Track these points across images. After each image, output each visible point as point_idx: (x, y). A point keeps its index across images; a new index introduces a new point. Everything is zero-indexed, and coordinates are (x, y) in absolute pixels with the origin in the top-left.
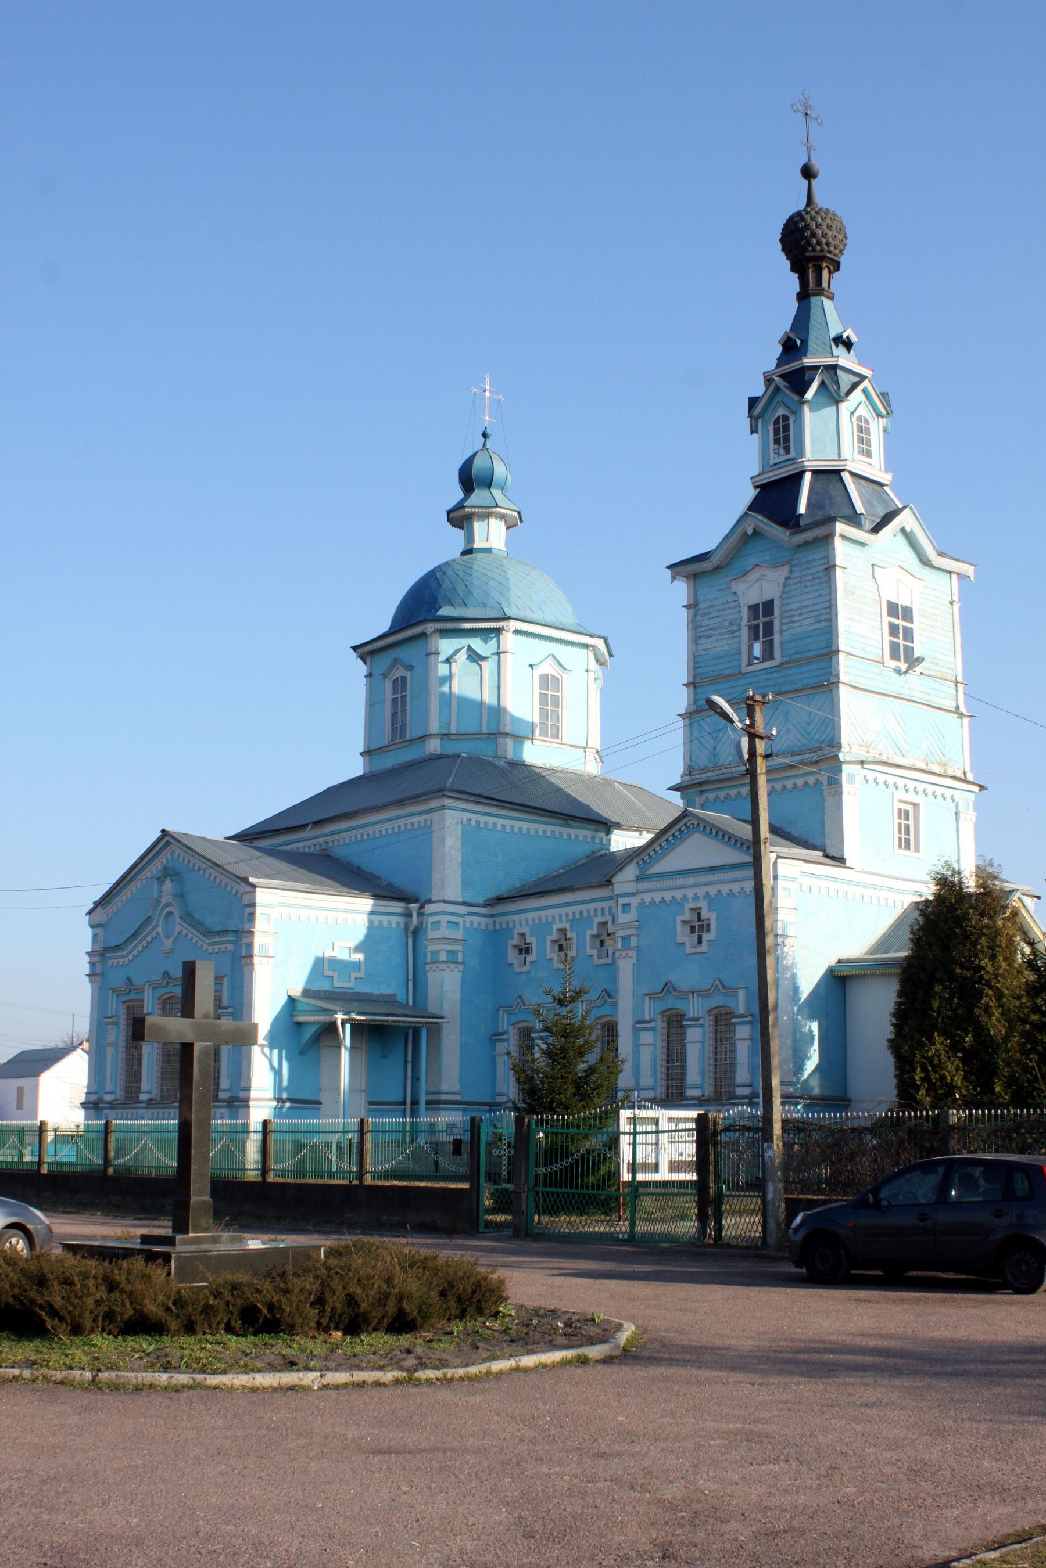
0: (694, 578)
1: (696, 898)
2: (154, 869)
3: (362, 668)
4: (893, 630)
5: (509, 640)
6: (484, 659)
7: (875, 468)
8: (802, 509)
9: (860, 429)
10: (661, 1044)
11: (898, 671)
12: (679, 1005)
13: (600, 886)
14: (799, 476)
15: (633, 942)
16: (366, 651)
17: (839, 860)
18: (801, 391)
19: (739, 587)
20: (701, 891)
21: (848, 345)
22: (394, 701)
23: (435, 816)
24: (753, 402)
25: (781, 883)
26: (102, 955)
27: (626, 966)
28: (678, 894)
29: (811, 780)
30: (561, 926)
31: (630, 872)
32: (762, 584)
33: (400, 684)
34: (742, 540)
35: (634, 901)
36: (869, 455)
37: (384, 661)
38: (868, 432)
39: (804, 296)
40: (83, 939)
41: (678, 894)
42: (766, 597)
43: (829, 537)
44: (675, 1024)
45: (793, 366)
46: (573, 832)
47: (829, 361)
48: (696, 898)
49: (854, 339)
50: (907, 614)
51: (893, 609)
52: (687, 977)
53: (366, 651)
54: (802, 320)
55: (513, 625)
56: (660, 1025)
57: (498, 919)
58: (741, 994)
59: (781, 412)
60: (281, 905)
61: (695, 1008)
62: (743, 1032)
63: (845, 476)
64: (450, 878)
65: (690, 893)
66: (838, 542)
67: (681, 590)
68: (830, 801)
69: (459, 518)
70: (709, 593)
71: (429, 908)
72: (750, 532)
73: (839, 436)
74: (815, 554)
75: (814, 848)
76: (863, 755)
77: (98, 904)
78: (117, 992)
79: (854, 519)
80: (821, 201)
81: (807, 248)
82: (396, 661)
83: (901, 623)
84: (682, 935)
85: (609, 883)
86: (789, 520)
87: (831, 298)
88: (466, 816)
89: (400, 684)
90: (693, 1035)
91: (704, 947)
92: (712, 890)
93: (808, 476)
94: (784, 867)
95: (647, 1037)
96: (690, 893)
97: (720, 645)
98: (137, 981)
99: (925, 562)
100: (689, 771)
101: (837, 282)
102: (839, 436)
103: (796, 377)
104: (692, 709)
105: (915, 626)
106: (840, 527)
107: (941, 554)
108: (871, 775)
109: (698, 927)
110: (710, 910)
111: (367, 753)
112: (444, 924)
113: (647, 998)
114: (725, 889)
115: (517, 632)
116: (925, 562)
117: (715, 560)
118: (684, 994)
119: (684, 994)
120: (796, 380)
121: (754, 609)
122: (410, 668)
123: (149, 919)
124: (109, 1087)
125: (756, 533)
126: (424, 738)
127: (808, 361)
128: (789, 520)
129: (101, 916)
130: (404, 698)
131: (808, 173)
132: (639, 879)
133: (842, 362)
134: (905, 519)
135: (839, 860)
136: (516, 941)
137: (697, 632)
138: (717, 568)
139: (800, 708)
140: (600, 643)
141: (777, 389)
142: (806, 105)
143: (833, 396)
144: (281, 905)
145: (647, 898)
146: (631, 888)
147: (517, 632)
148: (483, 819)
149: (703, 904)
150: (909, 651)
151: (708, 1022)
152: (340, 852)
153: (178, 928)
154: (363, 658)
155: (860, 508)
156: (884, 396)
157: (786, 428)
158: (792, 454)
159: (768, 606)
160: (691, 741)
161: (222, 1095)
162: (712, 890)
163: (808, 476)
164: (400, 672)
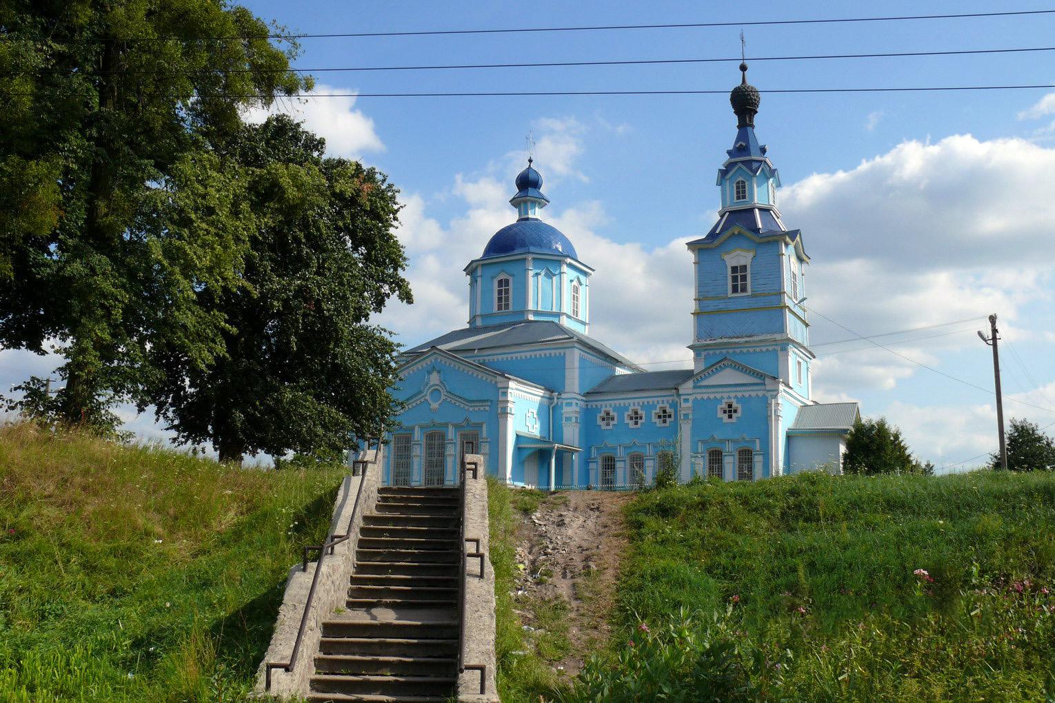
0: (700, 250)
1: (729, 397)
5: (565, 268)
6: (555, 275)
15: (690, 417)
19: (726, 257)
20: (732, 395)
22: (500, 292)
23: (567, 350)
24: (720, 170)
28: (718, 396)
30: (634, 408)
31: (690, 384)
33: (503, 283)
35: (691, 398)
42: (742, 263)
48: (729, 397)
55: (569, 260)
57: (590, 404)
58: (758, 441)
59: (740, 179)
60: (517, 389)
62: (758, 460)
64: (574, 383)
65: (725, 395)
69: (515, 202)
71: (563, 396)
72: (736, 233)
80: (749, 82)
81: (744, 104)
89: (503, 283)
92: (739, 395)
103: (745, 162)
104: (698, 311)
109: (636, 417)
110: (670, 408)
112: (574, 404)
113: (700, 444)
121: (734, 269)
123: (420, 392)
125: (740, 234)
130: (507, 292)
136: (603, 414)
144: (517, 389)
145: (699, 397)
146: (690, 392)
153: (443, 397)
157: (744, 187)
158: (747, 199)
159: (744, 268)
164: (503, 276)
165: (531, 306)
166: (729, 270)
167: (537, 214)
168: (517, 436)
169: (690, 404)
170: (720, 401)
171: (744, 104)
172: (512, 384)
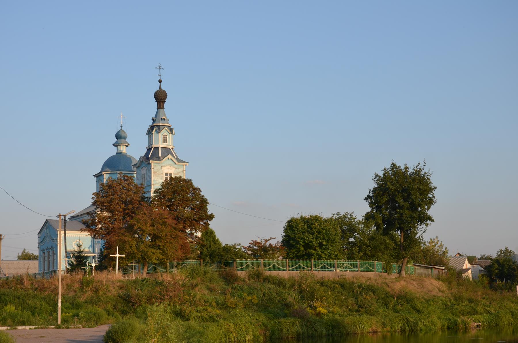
9: (164, 138)
18: (152, 130)
19: (142, 170)
26: (40, 243)
36: (167, 142)
40: (37, 240)
63: (160, 148)
66: (152, 164)
69: (116, 145)
73: (159, 140)
78: (42, 251)
80: (163, 88)
81: (160, 98)
101: (166, 105)
102: (159, 140)
120: (152, 127)
129: (40, 235)
131: (160, 81)
143: (158, 132)
154: (97, 177)
167: (123, 149)
171: (160, 98)
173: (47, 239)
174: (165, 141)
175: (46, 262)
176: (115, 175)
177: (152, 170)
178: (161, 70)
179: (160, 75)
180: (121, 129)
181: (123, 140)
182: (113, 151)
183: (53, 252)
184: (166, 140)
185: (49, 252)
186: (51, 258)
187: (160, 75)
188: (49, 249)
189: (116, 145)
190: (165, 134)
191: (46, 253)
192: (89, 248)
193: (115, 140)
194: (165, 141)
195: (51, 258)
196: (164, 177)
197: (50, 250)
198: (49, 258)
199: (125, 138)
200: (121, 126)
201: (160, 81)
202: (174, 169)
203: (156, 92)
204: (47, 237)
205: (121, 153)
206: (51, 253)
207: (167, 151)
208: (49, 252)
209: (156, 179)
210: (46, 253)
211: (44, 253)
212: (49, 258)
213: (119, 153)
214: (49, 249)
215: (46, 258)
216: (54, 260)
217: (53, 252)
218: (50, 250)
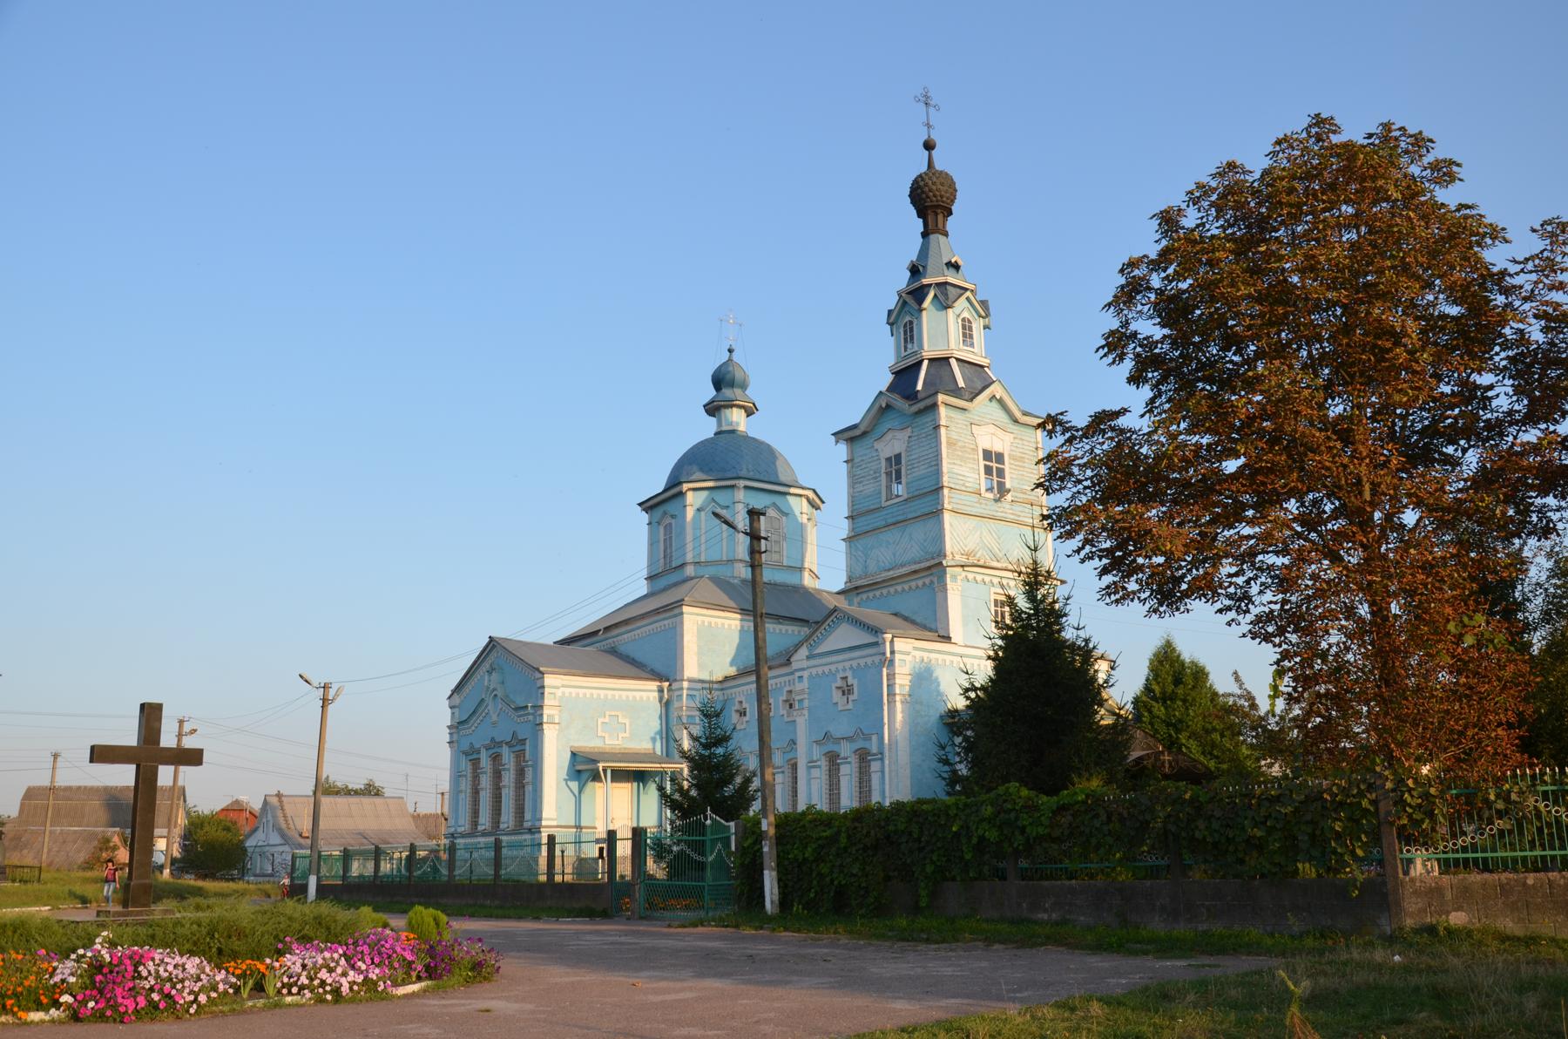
2: (486, 666)
3: (645, 517)
4: (988, 470)
7: (977, 354)
8: (919, 387)
9: (964, 327)
10: (825, 777)
11: (996, 501)
12: (835, 748)
13: (781, 665)
14: (920, 363)
15: (806, 703)
16: (649, 506)
17: (946, 638)
18: (920, 301)
20: (847, 664)
21: (956, 267)
24: (890, 312)
25: (898, 657)
26: (457, 727)
27: (802, 722)
29: (927, 581)
32: (893, 443)
33: (668, 528)
34: (881, 410)
35: (806, 674)
36: (972, 345)
37: (658, 512)
38: (970, 329)
39: (925, 235)
40: (445, 717)
41: (833, 668)
43: (934, 406)
44: (833, 760)
45: (916, 285)
46: (784, 628)
47: (941, 279)
49: (960, 263)
50: (1000, 458)
51: (987, 455)
52: (841, 728)
53: (649, 506)
54: (924, 252)
56: (824, 763)
59: (908, 318)
61: (846, 750)
63: (953, 362)
66: (943, 410)
67: (842, 450)
68: (939, 595)
69: (713, 409)
70: (861, 449)
74: (926, 419)
75: (930, 630)
76: (964, 560)
77: (454, 692)
78: (466, 754)
79: (956, 392)
80: (939, 166)
81: (931, 201)
82: (665, 513)
83: (994, 465)
84: (837, 696)
85: (788, 662)
86: (911, 396)
87: (946, 235)
88: (700, 618)
89: (668, 528)
90: (845, 769)
91: (850, 706)
93: (926, 363)
94: (900, 644)
95: (815, 773)
96: (840, 666)
97: (869, 488)
98: (477, 746)
99: (1016, 421)
100: (850, 579)
101: (951, 223)
105: (1007, 467)
106: (941, 397)
107: (1025, 414)
108: (970, 576)
111: (650, 578)
114: (862, 662)
115: (746, 487)
116: (1016, 421)
117: (862, 428)
118: (838, 740)
119: (838, 740)
120: (916, 294)
121: (888, 460)
122: (673, 517)
124: (461, 822)
125: (888, 406)
126: (683, 565)
127: (925, 281)
128: (911, 396)
129: (457, 700)
131: (929, 146)
132: (808, 658)
133: (950, 280)
134: (996, 389)
135: (946, 638)
136: (737, 707)
137: (854, 480)
138: (864, 434)
139: (918, 531)
140: (811, 494)
141: (905, 303)
142: (927, 97)
143: (944, 304)
146: (805, 664)
147: (746, 487)
148: (713, 620)
149: (849, 674)
150: (1001, 485)
151: (854, 760)
152: (622, 649)
154: (646, 510)
155: (961, 384)
156: (984, 303)
157: (912, 330)
159: (898, 457)
160: (851, 555)
161: (526, 825)
162: (854, 663)
163: (926, 363)
165: (689, 557)
166: (883, 463)
167: (737, 417)
168: (574, 754)
169: (805, 684)
170: (832, 674)
171: (931, 201)
172: (549, 680)
173: (492, 708)
174: (967, 334)
175: (485, 797)
176: (729, 492)
177: (943, 431)
178: (931, 110)
179: (928, 126)
180: (730, 360)
181: (738, 391)
182: (707, 427)
183: (520, 755)
184: (971, 337)
185: (496, 758)
186: (508, 779)
187: (928, 126)
188: (500, 744)
189: (713, 409)
190: (966, 315)
191: (485, 762)
192: (654, 740)
193: (711, 392)
194: (967, 334)
195: (508, 779)
196: (982, 463)
197: (505, 751)
198: (497, 775)
199: (744, 386)
200: (730, 351)
201: (929, 146)
202: (1008, 438)
203: (915, 182)
204: (489, 700)
205: (733, 432)
206: (508, 757)
207: (979, 380)
208: (496, 758)
209: (957, 469)
210: (485, 762)
211: (476, 763)
212: (497, 775)
213: (727, 434)
214: (500, 744)
215: (486, 782)
216: (520, 786)
217: (520, 755)
218: (505, 751)
